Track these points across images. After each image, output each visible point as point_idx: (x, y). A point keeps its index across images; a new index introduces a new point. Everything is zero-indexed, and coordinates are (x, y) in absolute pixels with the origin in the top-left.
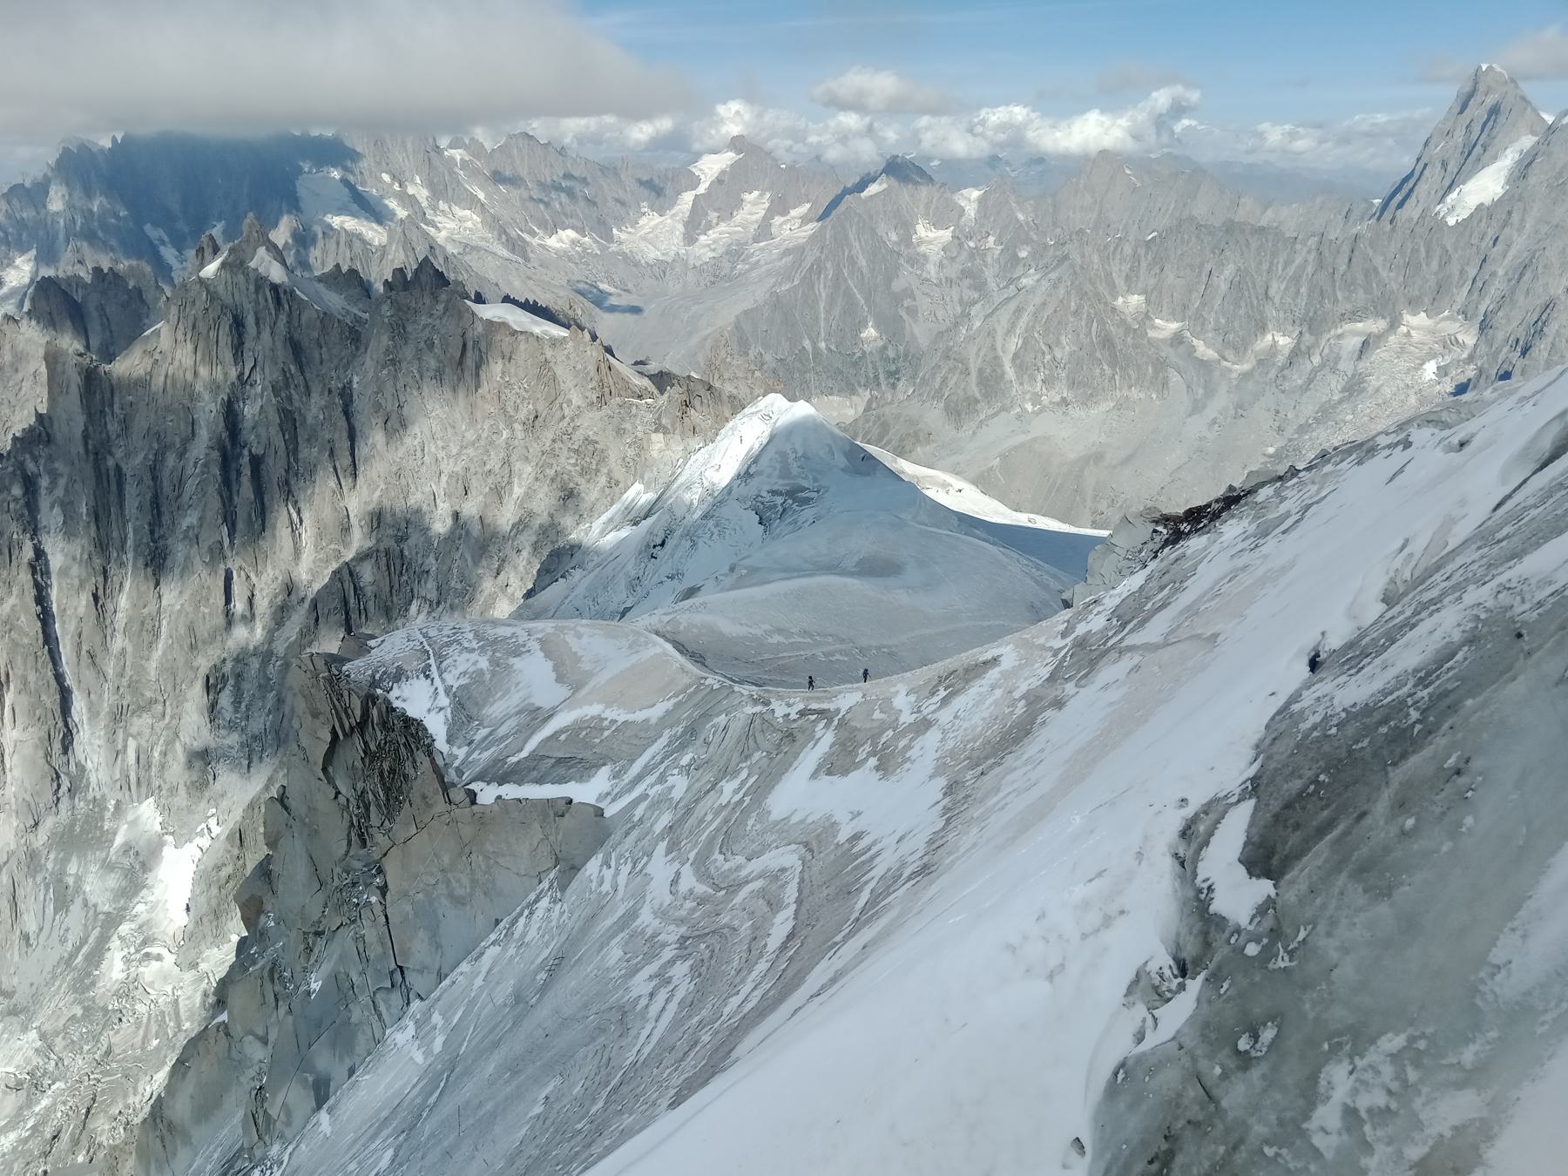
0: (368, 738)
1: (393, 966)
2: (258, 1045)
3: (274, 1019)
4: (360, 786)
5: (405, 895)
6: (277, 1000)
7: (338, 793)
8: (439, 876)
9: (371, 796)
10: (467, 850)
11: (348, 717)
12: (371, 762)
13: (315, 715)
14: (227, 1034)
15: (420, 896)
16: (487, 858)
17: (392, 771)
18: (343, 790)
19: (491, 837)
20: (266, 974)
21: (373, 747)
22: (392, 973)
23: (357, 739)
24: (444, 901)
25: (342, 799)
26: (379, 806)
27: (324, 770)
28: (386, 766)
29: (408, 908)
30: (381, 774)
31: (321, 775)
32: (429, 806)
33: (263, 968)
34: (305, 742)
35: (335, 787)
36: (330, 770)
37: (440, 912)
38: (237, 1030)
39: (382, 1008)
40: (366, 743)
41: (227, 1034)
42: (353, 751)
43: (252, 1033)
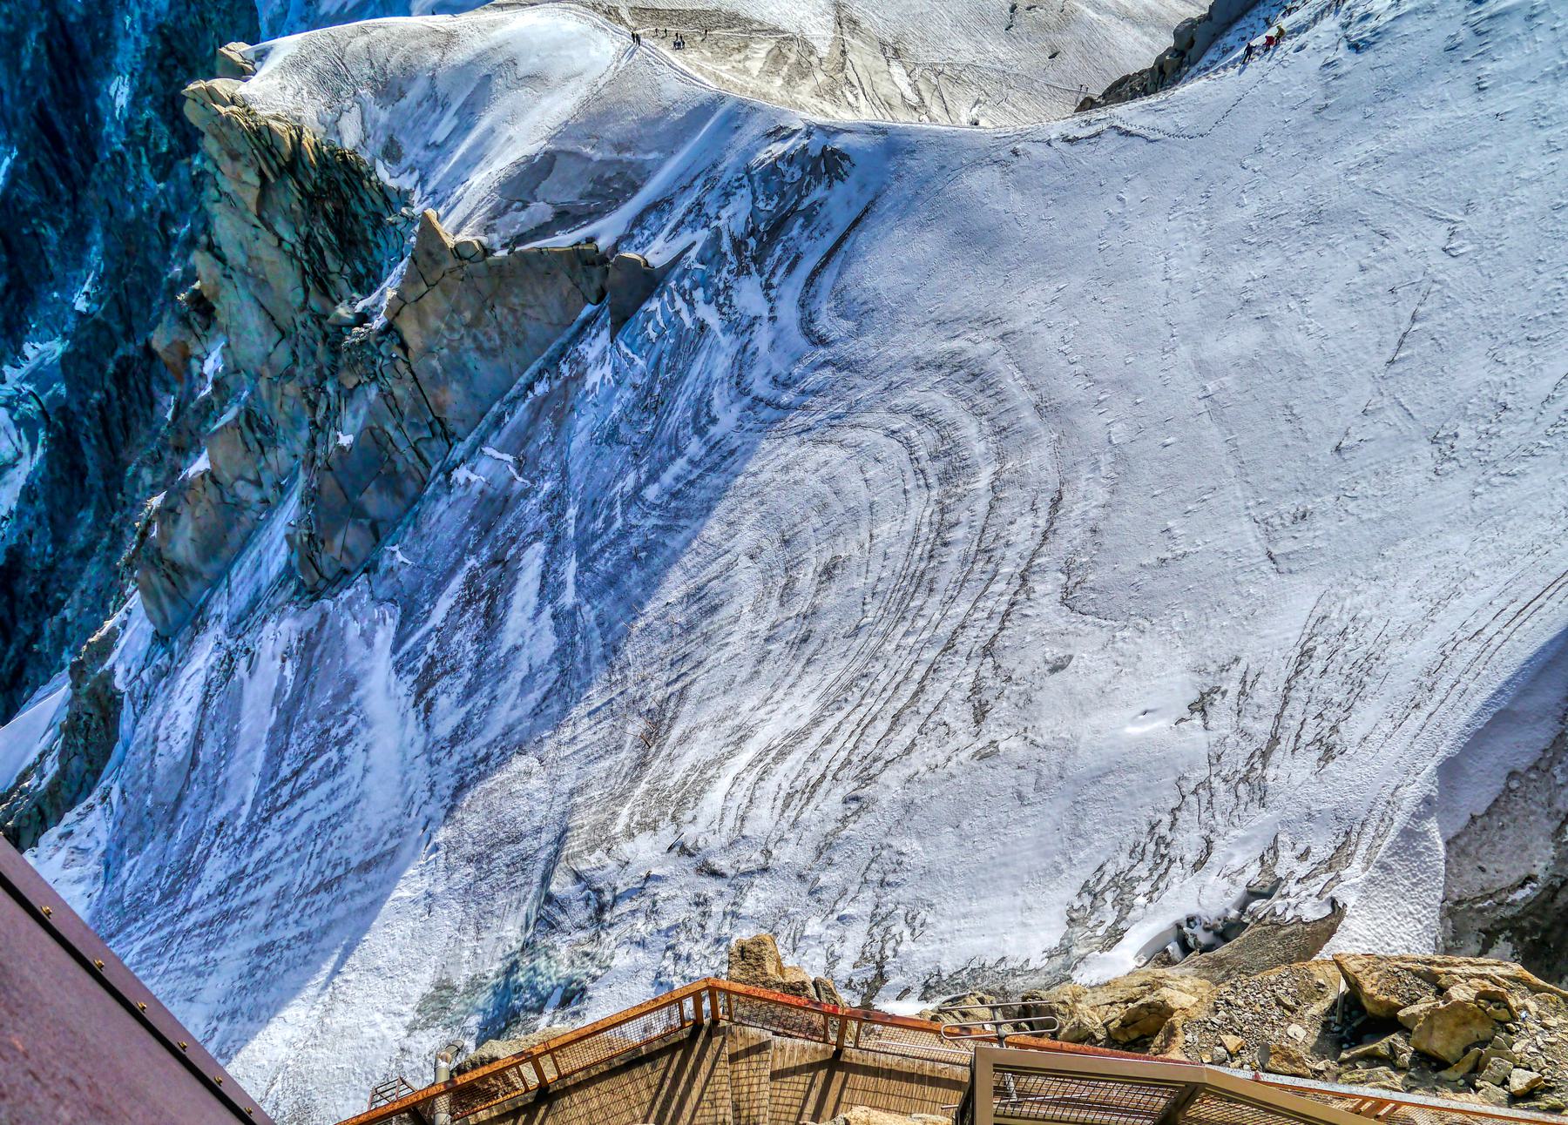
0: (300, 177)
1: (431, 418)
2: (251, 488)
3: (263, 464)
4: (303, 229)
5: (428, 351)
6: (262, 447)
7: (281, 240)
8: (463, 331)
9: (320, 240)
10: (489, 302)
11: (274, 157)
12: (310, 204)
13: (235, 157)
14: (215, 482)
15: (445, 351)
16: (513, 311)
17: (337, 212)
18: (286, 236)
19: (516, 291)
20: (242, 421)
21: (309, 187)
22: (431, 425)
23: (291, 183)
24: (473, 355)
25: (287, 247)
26: (333, 251)
27: (259, 217)
28: (329, 206)
29: (435, 363)
30: (326, 215)
31: (257, 222)
32: (437, 263)
33: (237, 419)
34: (227, 186)
35: (276, 234)
36: (265, 215)
37: (471, 365)
38: (226, 476)
39: (426, 455)
40: (300, 183)
41: (215, 482)
42: (289, 196)
43: (240, 477)
